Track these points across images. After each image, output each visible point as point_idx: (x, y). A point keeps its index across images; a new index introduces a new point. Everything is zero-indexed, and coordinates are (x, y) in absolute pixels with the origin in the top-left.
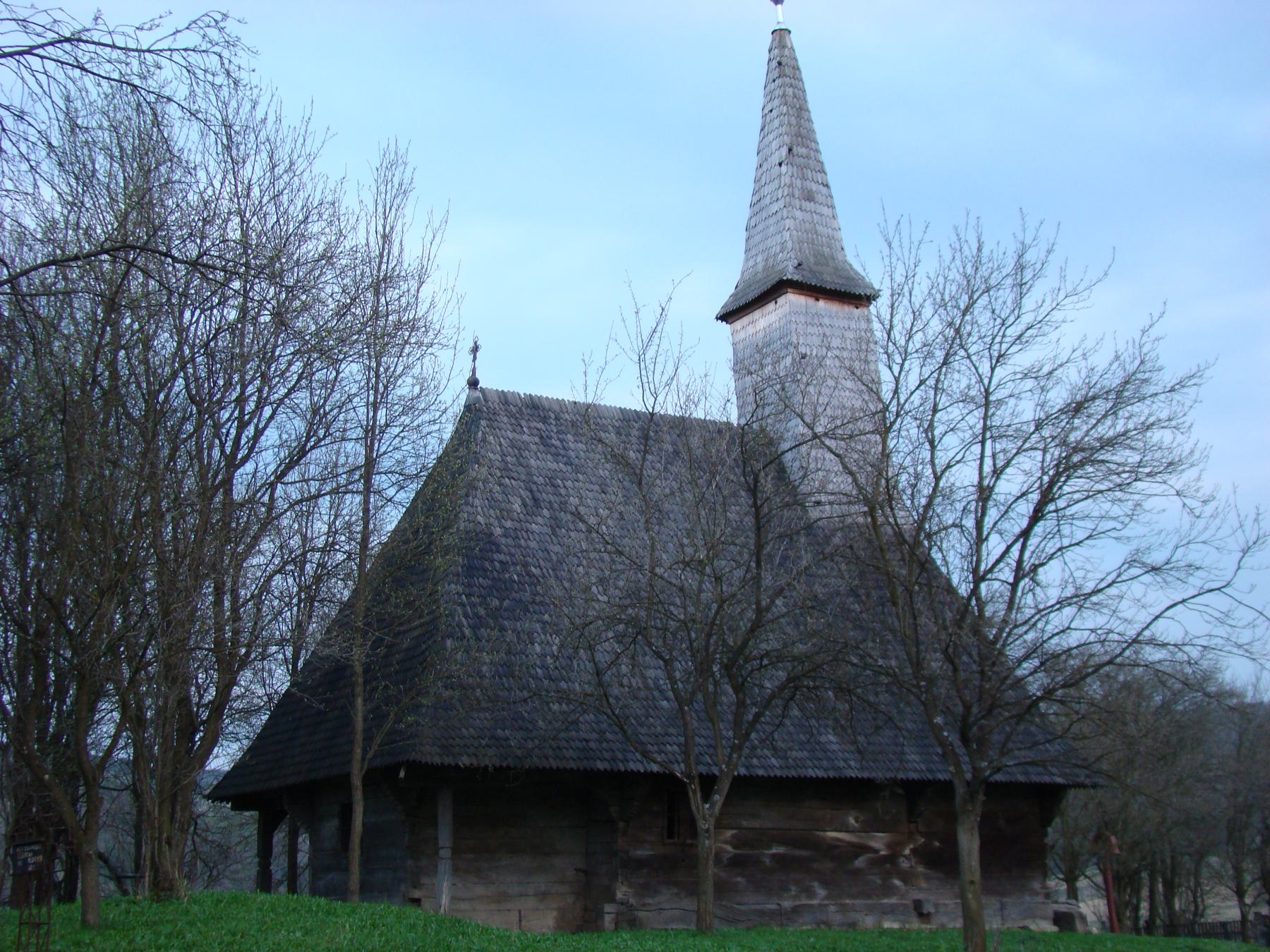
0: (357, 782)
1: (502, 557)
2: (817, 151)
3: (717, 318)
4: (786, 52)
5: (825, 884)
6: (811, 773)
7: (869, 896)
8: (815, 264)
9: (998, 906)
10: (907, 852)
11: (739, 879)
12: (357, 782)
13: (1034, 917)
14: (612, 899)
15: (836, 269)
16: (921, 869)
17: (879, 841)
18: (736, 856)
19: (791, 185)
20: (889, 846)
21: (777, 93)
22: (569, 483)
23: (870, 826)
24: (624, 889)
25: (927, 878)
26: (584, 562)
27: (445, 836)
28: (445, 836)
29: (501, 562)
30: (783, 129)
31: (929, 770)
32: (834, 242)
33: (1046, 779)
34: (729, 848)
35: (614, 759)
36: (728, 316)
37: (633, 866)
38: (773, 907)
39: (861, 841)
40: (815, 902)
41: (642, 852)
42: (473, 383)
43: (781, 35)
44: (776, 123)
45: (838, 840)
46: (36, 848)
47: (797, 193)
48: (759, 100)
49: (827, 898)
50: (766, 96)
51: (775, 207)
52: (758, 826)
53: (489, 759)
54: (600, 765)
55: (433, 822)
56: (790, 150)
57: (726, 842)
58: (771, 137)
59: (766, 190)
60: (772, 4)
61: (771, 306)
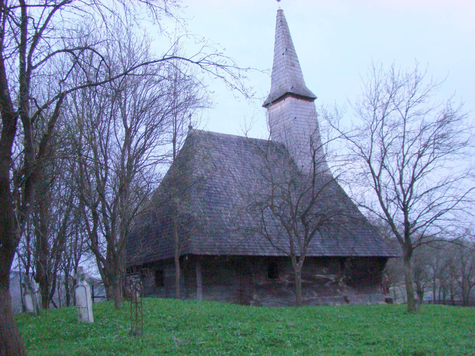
0: (177, 261)
1: (208, 185)
2: (294, 50)
3: (263, 106)
4: (283, 17)
5: (317, 292)
6: (314, 255)
8: (297, 87)
10: (341, 280)
12: (177, 261)
13: (379, 300)
14: (252, 299)
15: (303, 89)
16: (345, 286)
17: (332, 277)
19: (287, 61)
20: (335, 279)
21: (280, 31)
22: (225, 161)
23: (329, 273)
24: (256, 295)
26: (234, 187)
27: (199, 279)
28: (199, 279)
29: (208, 187)
30: (284, 43)
31: (349, 253)
32: (302, 79)
33: (383, 255)
34: (287, 281)
35: (254, 252)
36: (266, 105)
37: (258, 288)
40: (314, 298)
41: (261, 283)
42: (190, 127)
43: (280, 12)
44: (281, 40)
46: (136, 276)
47: (289, 64)
48: (274, 34)
49: (318, 296)
50: (276, 32)
51: (282, 69)
53: (216, 252)
54: (250, 254)
55: (195, 275)
56: (286, 49)
57: (286, 279)
58: (279, 45)
59: (279, 63)
60: (277, 2)
61: (283, 101)
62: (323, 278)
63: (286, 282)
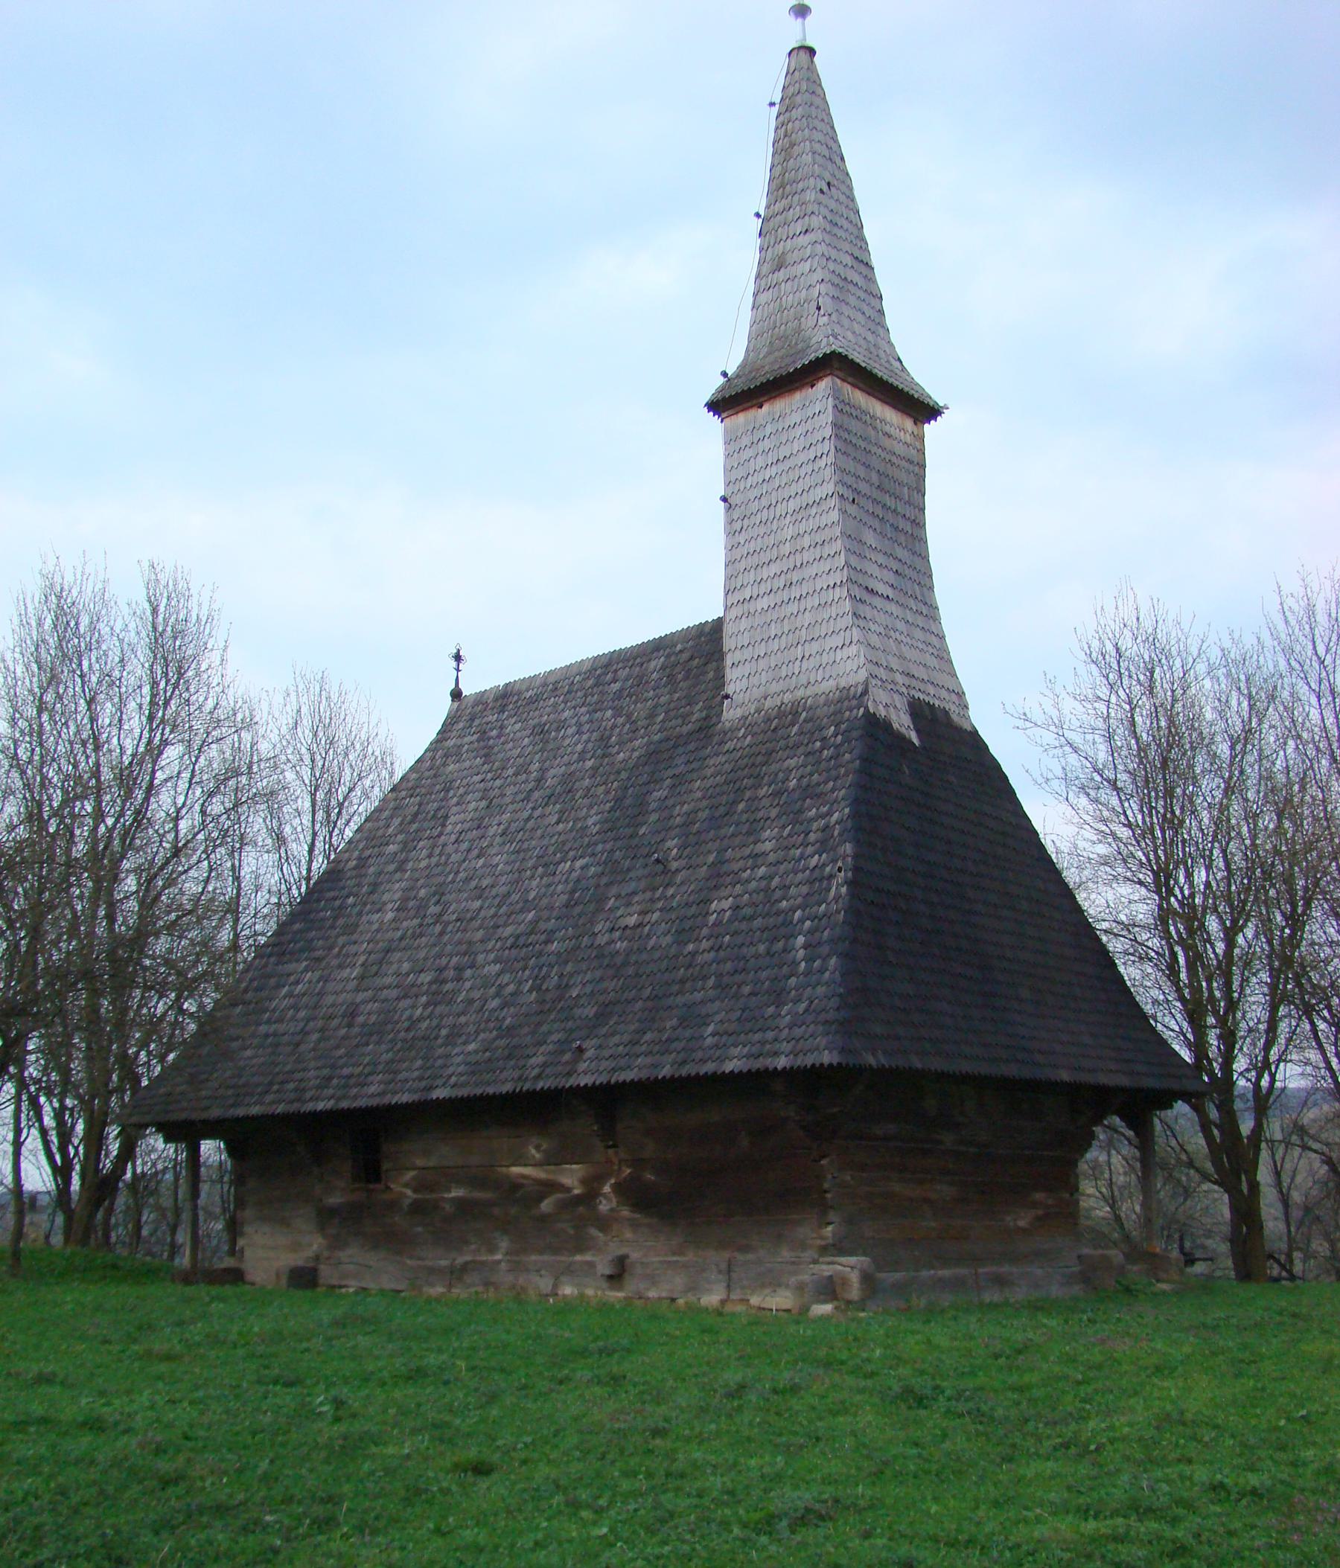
7: (556, 1250)
9: (724, 1266)
10: (607, 1189)
11: (420, 1229)
16: (625, 1212)
17: (571, 1177)
18: (416, 1201)
20: (583, 1182)
23: (554, 1159)
25: (635, 1225)
34: (409, 1192)
38: (444, 1263)
39: (551, 1177)
41: (334, 1200)
45: (523, 1176)
52: (431, 1164)
57: (407, 1185)
63: (403, 1195)
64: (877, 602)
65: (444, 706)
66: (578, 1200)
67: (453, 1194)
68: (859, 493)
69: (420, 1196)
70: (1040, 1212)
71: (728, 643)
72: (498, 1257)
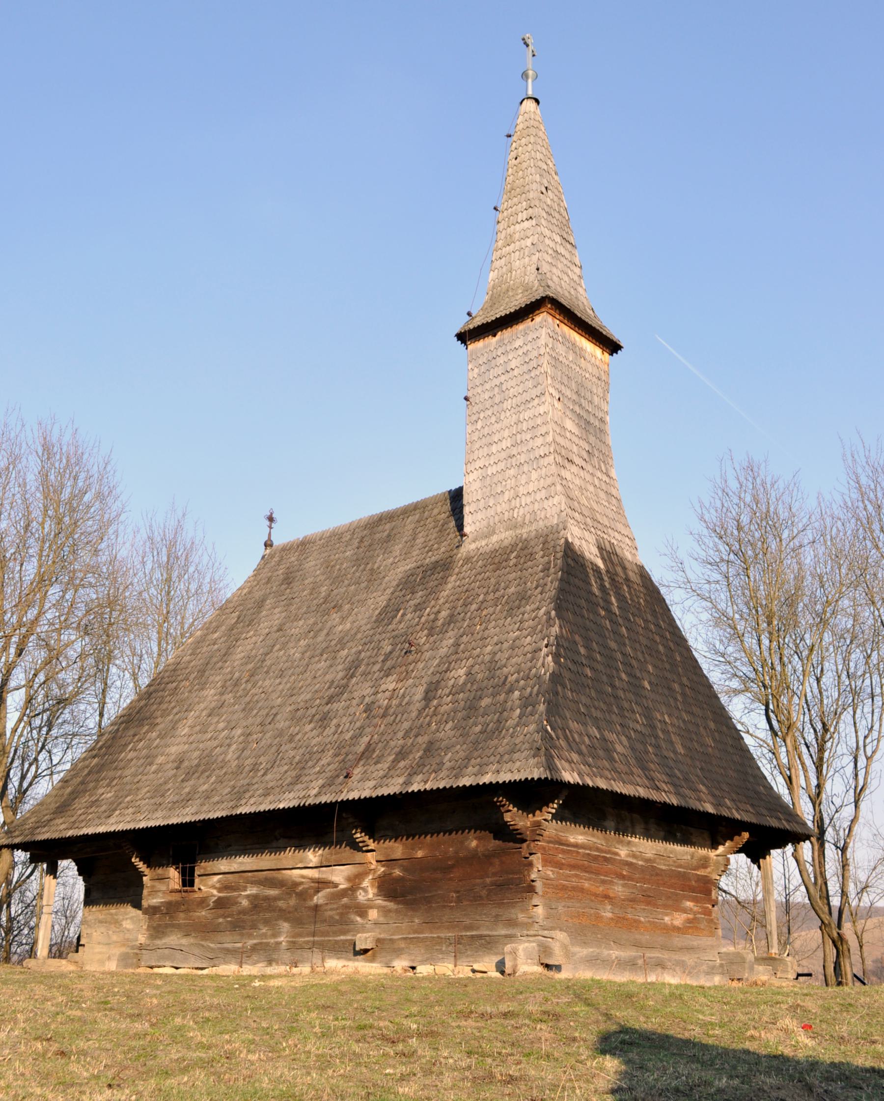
11: (221, 920)
16: (380, 902)
17: (339, 876)
18: (219, 898)
20: (349, 879)
34: (215, 892)
39: (324, 876)
45: (303, 877)
57: (213, 887)
62: (313, 880)
64: (574, 469)
65: (261, 551)
66: (344, 893)
67: (248, 892)
68: (563, 394)
69: (221, 895)
70: (691, 916)
71: (466, 499)
72: (282, 939)
